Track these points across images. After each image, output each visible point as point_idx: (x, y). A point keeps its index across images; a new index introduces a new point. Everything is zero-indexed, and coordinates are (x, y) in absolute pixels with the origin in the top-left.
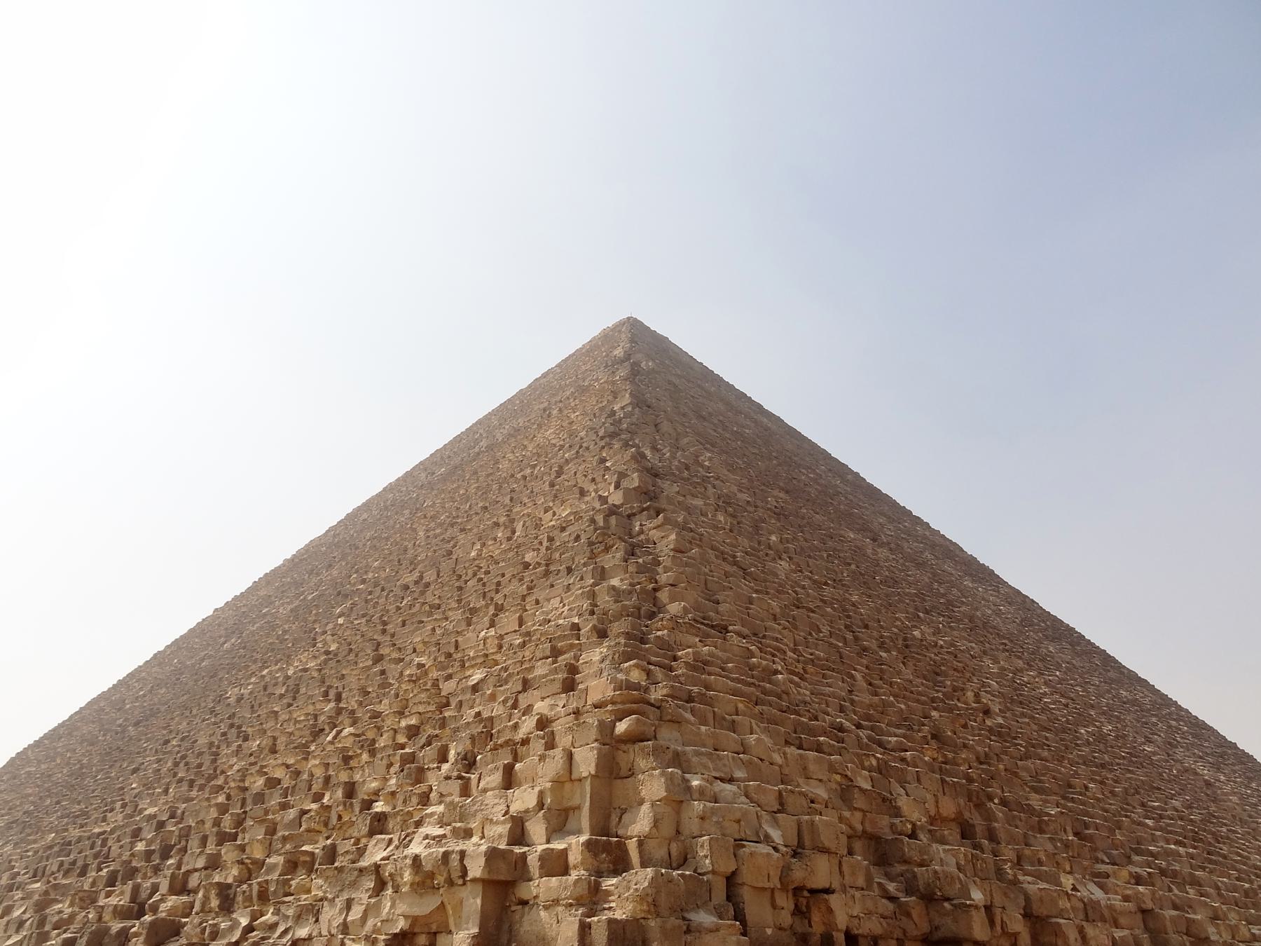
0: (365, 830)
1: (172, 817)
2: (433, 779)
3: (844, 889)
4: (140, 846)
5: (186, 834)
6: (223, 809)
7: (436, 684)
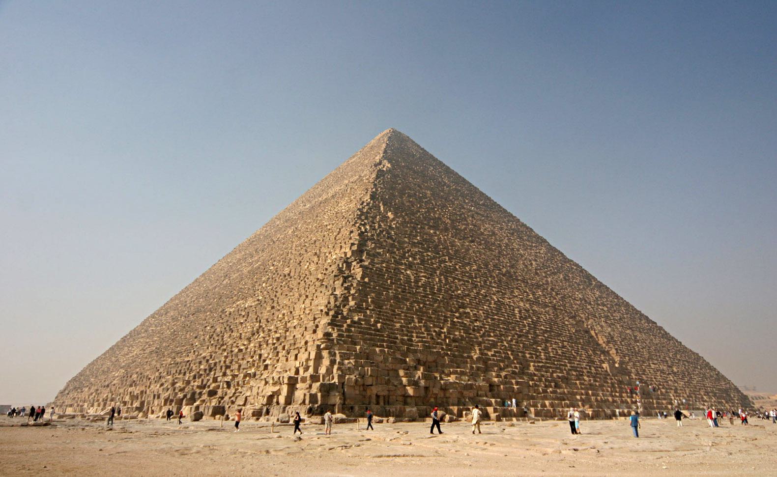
0: (263, 369)
1: (211, 358)
2: (280, 355)
3: (376, 384)
4: (202, 367)
5: (215, 364)
6: (226, 357)
7: (286, 324)
